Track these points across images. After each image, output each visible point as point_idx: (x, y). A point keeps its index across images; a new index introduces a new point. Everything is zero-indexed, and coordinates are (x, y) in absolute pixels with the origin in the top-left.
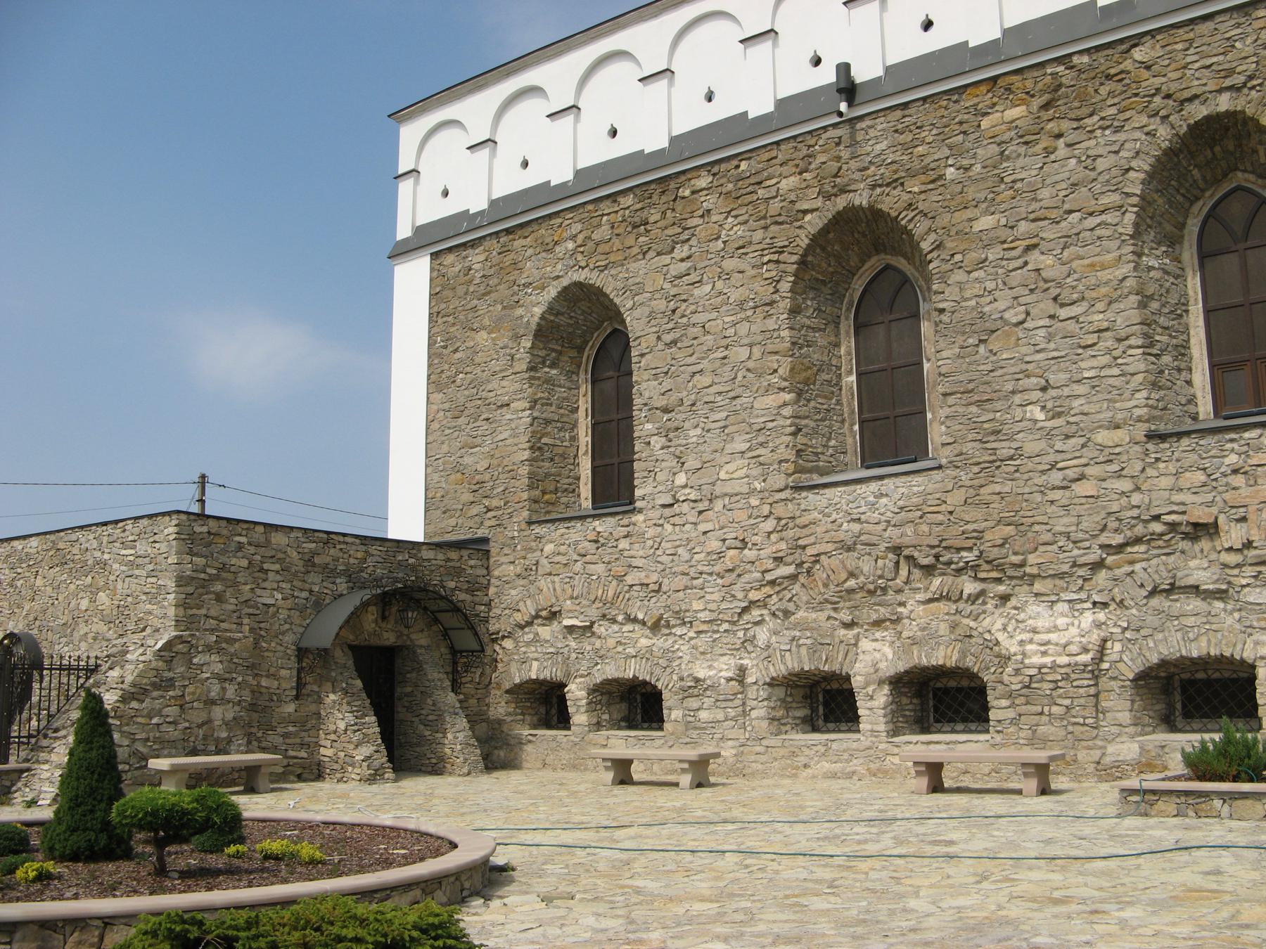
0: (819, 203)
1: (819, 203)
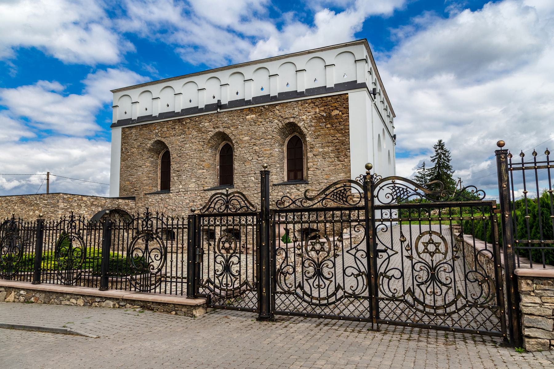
1: (213, 130)
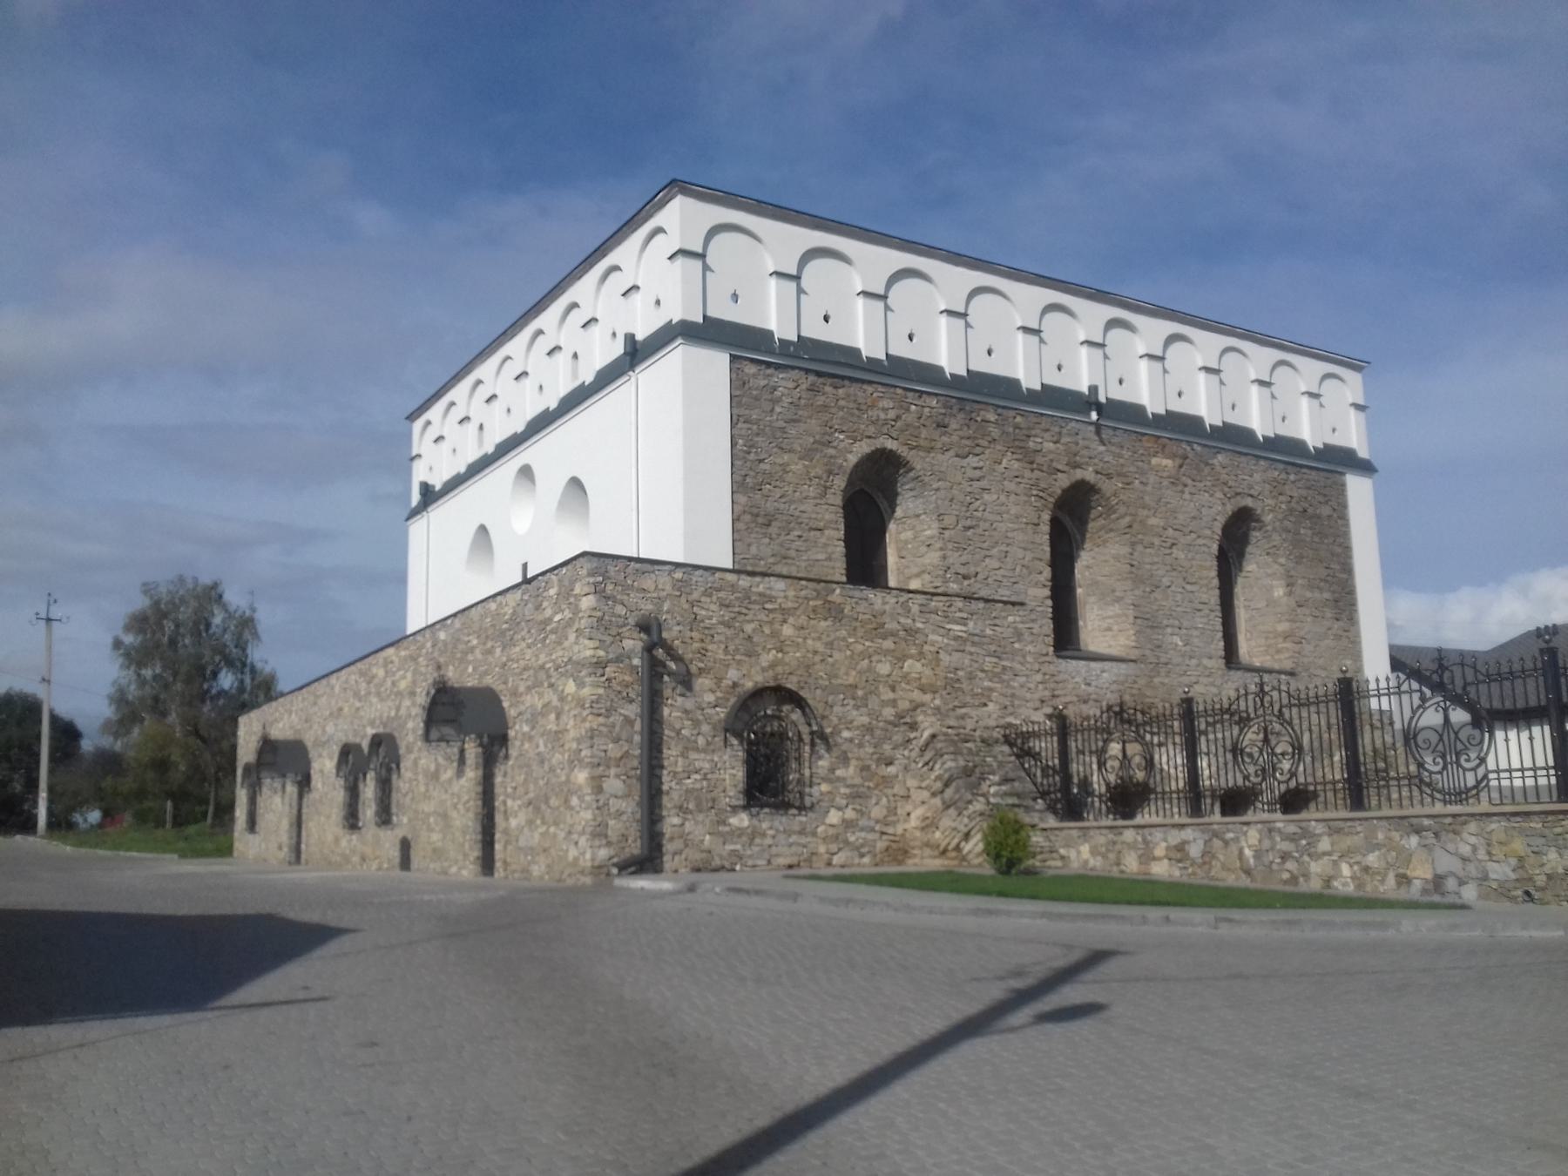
0: (1066, 468)
1: (1066, 468)
